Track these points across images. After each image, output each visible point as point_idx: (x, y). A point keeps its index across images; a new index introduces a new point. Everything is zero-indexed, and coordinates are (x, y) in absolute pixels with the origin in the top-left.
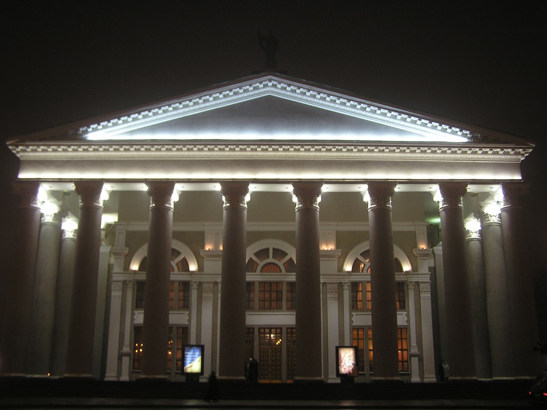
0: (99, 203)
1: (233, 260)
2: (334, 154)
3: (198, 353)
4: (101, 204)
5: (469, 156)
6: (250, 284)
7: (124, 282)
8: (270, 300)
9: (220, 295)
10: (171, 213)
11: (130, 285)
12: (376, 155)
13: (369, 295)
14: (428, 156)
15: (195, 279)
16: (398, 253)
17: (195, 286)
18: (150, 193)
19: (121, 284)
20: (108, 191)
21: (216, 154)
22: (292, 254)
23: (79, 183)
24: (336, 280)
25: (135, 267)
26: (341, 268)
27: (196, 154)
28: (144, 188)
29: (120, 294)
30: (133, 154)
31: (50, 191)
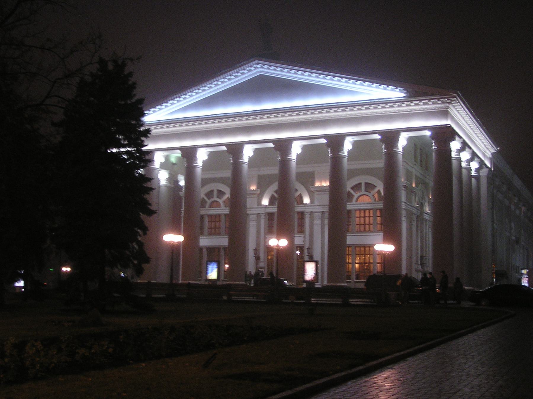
0: (398, 149)
1: (337, 195)
2: (302, 117)
3: (215, 266)
4: (346, 154)
5: (404, 108)
6: (349, 212)
7: (323, 212)
8: (365, 224)
9: (326, 221)
10: (345, 160)
11: (263, 216)
12: (332, 114)
13: (379, 218)
14: (372, 111)
15: (308, 210)
16: (301, 190)
17: (307, 216)
18: (433, 137)
19: (320, 214)
20: (350, 142)
21: (224, 124)
22: (380, 187)
23: (275, 142)
24: (255, 211)
25: (265, 202)
26: (259, 203)
27: (211, 125)
28: (224, 148)
29: (319, 221)
30: (172, 129)
31: (163, 156)
